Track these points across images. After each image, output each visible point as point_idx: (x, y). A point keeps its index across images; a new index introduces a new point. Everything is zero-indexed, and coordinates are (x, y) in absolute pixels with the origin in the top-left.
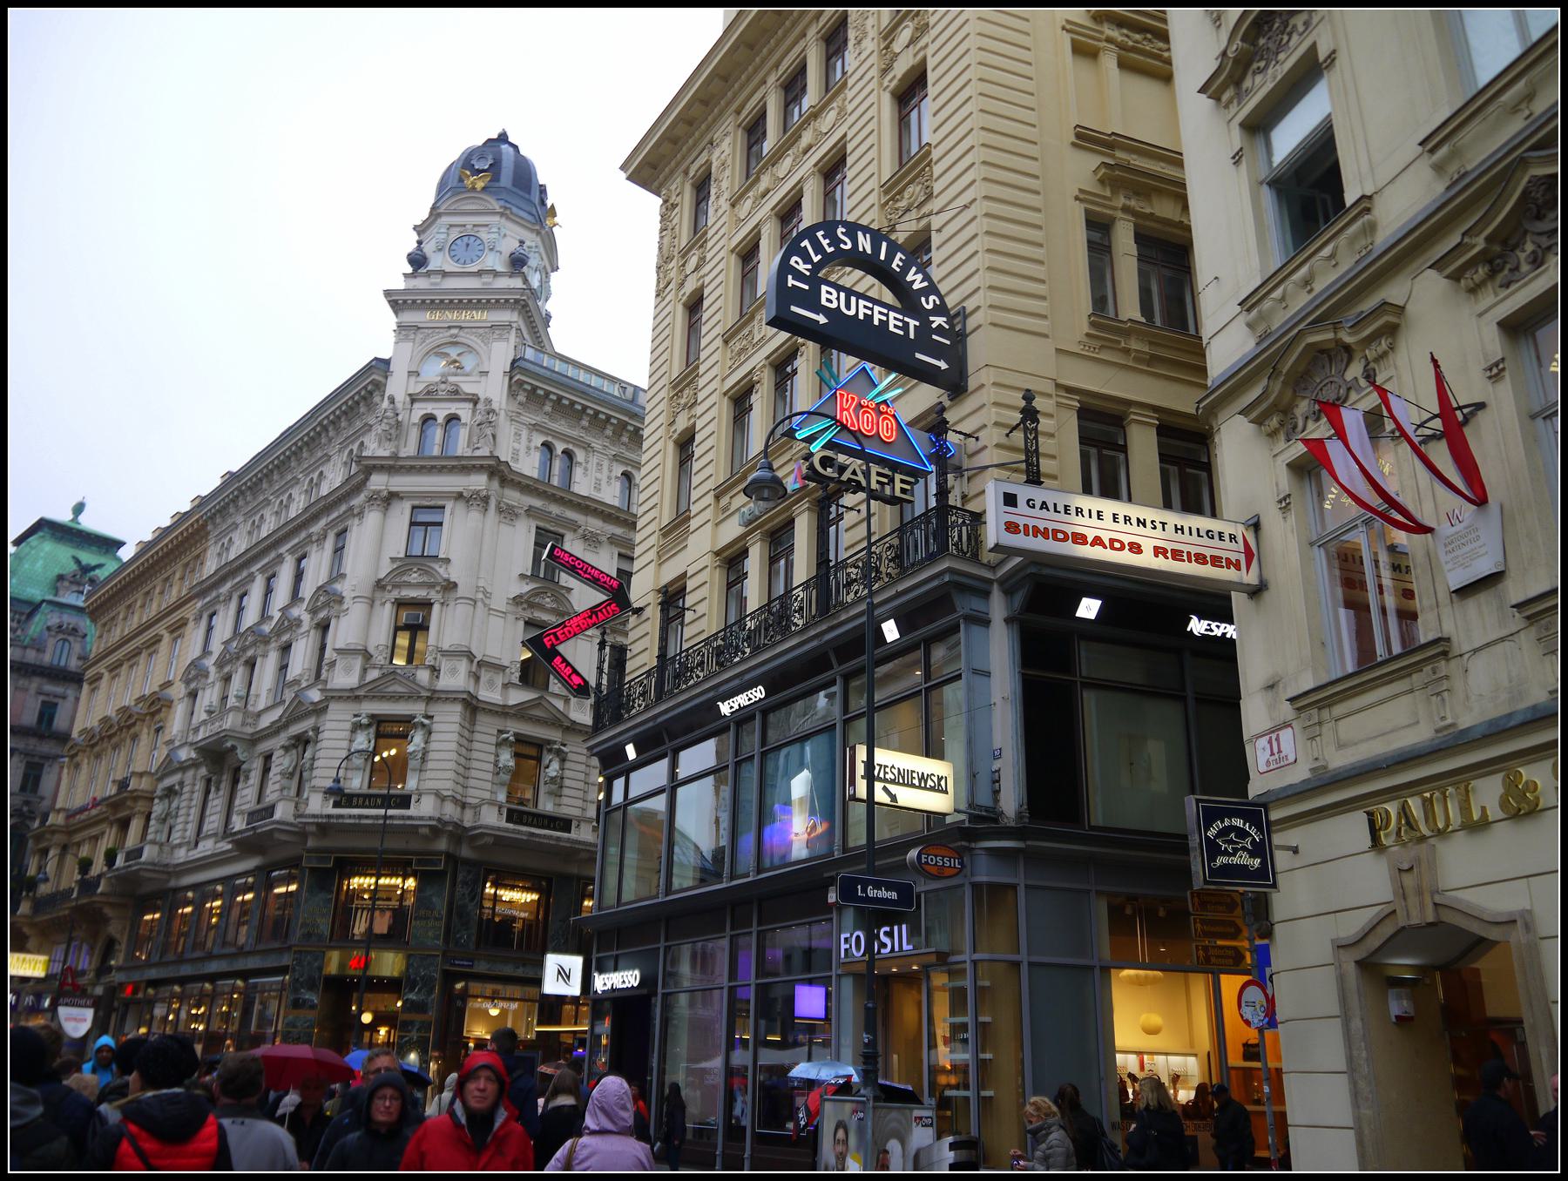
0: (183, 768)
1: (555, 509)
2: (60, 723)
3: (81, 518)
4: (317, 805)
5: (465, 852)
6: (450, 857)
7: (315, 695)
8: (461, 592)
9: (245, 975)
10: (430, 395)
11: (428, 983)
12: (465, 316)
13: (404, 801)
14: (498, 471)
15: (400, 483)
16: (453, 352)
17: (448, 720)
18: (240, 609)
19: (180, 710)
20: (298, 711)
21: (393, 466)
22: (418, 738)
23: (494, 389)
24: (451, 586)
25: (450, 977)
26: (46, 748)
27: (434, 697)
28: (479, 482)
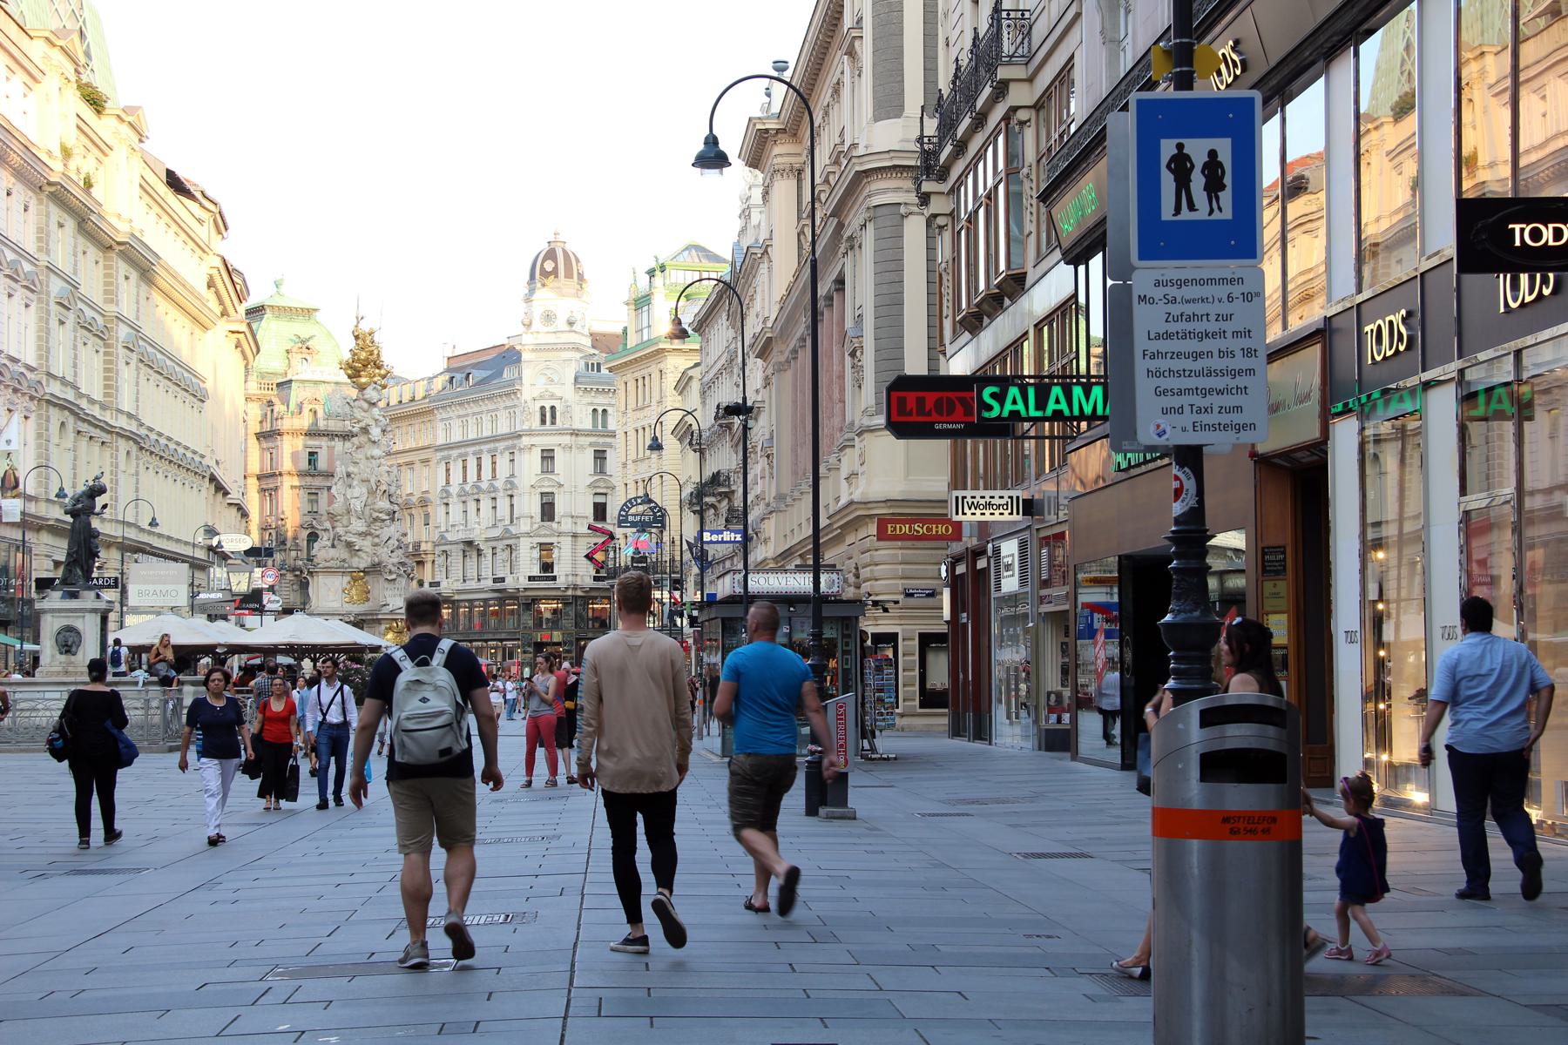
0: (451, 543)
1: (601, 440)
2: (322, 464)
3: (283, 289)
4: (523, 583)
5: (579, 593)
6: (576, 597)
7: (513, 530)
8: (566, 488)
9: (501, 640)
10: (542, 397)
11: (571, 643)
12: (550, 355)
13: (554, 578)
14: (575, 433)
15: (535, 440)
16: (548, 372)
17: (566, 542)
18: (465, 468)
19: (438, 513)
20: (506, 534)
21: (531, 433)
22: (556, 551)
23: (567, 391)
24: (561, 485)
25: (578, 640)
26: (318, 482)
27: (560, 534)
28: (567, 440)
